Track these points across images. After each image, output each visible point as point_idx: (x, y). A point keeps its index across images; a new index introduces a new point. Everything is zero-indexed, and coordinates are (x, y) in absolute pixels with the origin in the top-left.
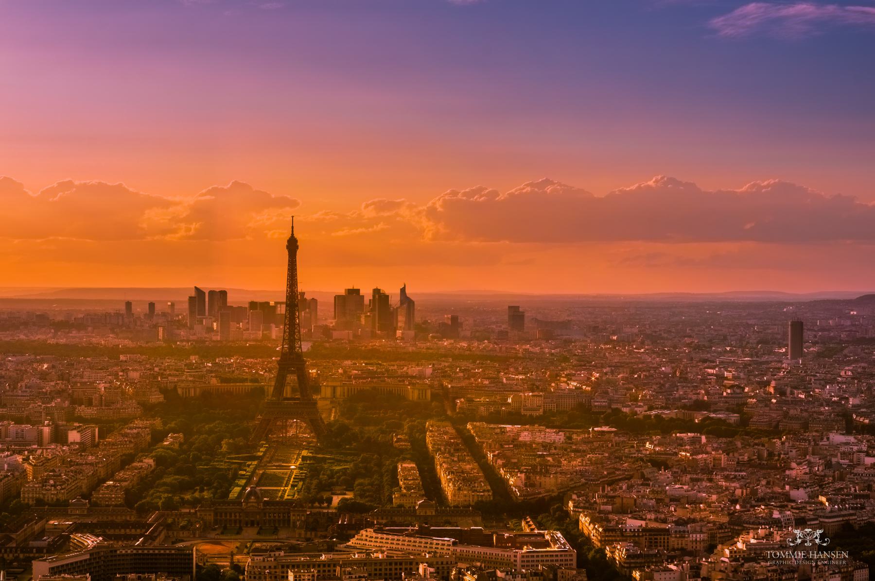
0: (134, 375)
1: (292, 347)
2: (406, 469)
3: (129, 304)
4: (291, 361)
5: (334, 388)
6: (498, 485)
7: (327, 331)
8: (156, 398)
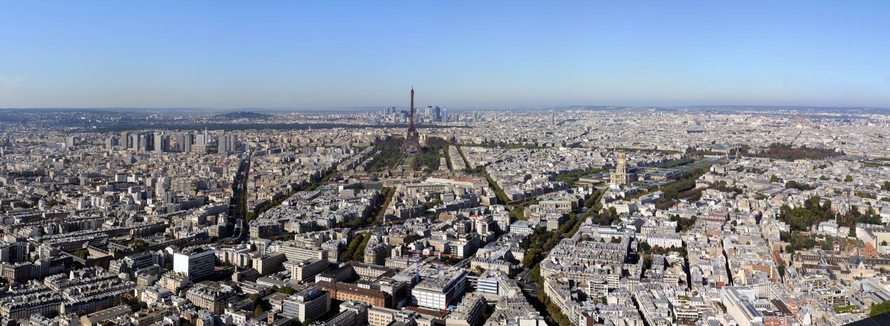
0: (369, 134)
2: (443, 160)
4: (412, 128)
6: (467, 165)
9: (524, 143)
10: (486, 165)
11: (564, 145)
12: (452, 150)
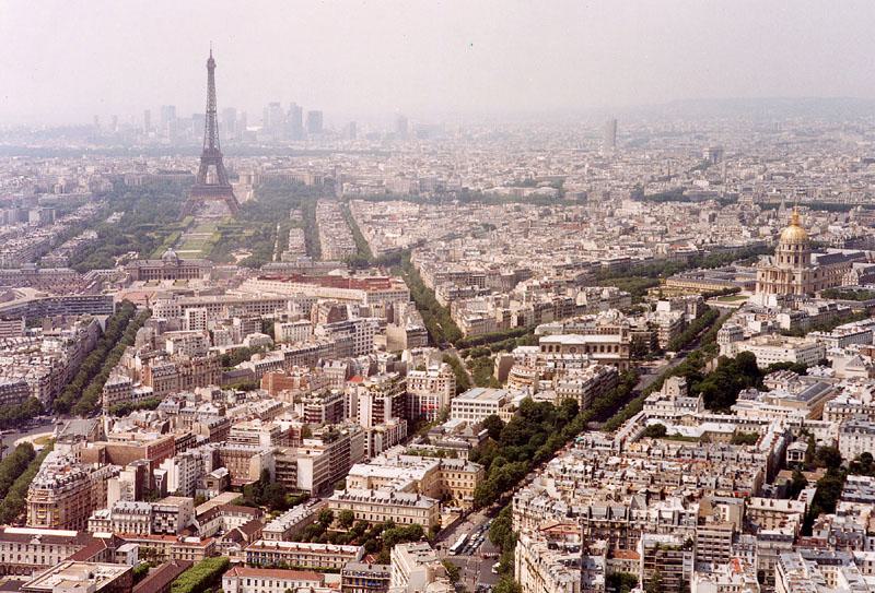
1: (211, 145)
2: (297, 239)
3: (96, 118)
4: (212, 156)
5: (250, 177)
6: (362, 245)
7: (252, 135)
8: (105, 185)
9: (527, 192)
10: (411, 247)
11: (638, 195)
12: (324, 209)
